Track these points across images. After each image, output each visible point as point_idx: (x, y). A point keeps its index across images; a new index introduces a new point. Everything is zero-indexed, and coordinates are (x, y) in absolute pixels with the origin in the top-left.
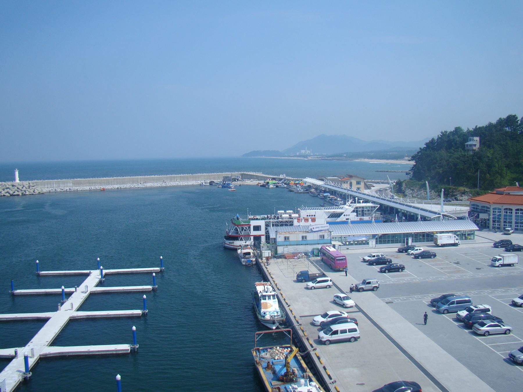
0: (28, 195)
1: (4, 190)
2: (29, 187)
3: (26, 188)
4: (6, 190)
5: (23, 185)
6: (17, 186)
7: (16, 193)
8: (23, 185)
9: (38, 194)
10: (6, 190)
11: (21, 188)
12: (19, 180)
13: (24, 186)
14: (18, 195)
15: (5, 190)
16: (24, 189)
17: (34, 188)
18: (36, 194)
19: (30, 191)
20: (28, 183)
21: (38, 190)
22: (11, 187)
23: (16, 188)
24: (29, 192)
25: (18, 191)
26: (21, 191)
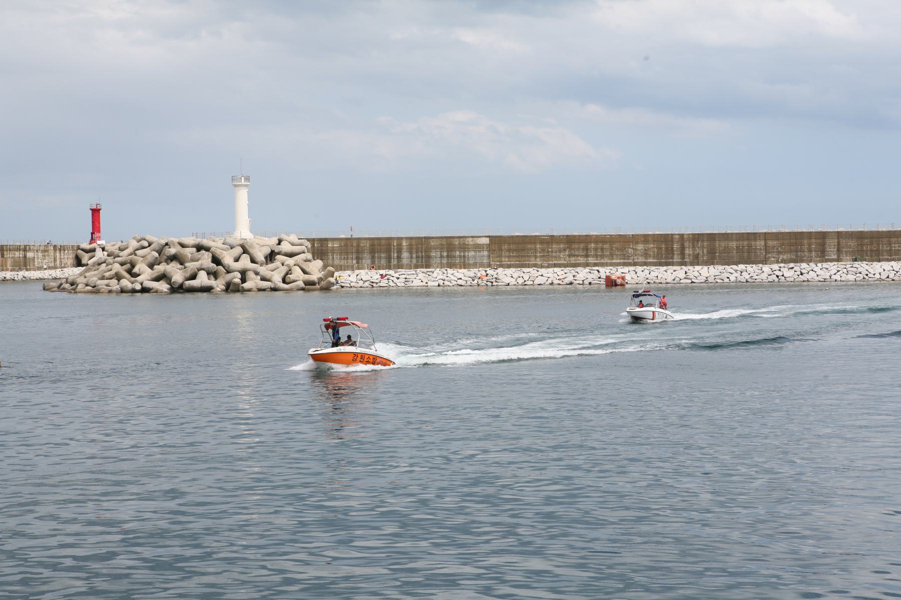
0: (249, 290)
1: (151, 266)
2: (271, 257)
3: (253, 261)
4: (160, 268)
5: (242, 246)
6: (212, 249)
7: (203, 279)
8: (242, 246)
9: (303, 289)
10: (160, 268)
11: (228, 260)
12: (251, 231)
13: (244, 253)
14: (208, 289)
15: (156, 267)
16: (245, 262)
17: (290, 261)
18: (291, 290)
19: (268, 277)
20: (275, 240)
21: (305, 272)
22: (189, 252)
23: (206, 259)
24: (263, 279)
25: (214, 275)
26: (228, 272)
